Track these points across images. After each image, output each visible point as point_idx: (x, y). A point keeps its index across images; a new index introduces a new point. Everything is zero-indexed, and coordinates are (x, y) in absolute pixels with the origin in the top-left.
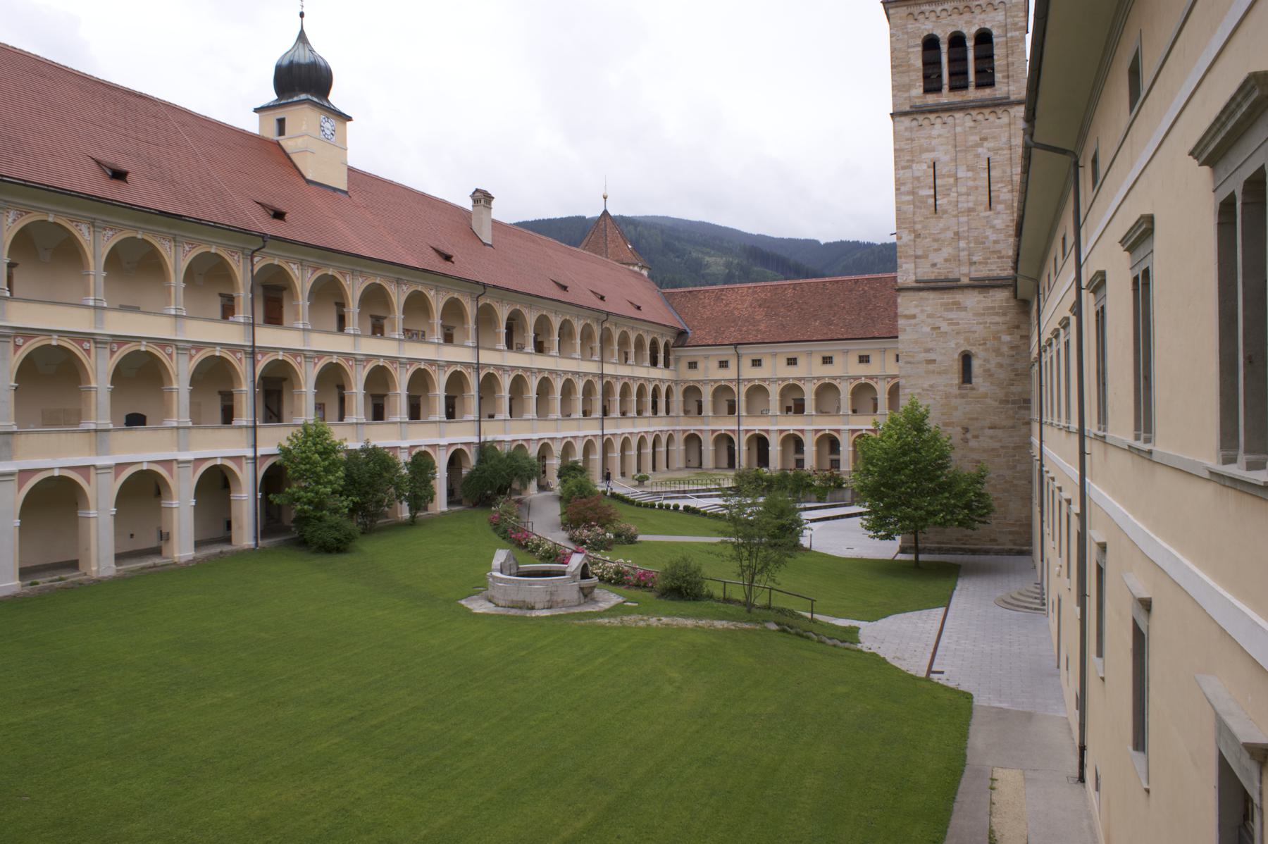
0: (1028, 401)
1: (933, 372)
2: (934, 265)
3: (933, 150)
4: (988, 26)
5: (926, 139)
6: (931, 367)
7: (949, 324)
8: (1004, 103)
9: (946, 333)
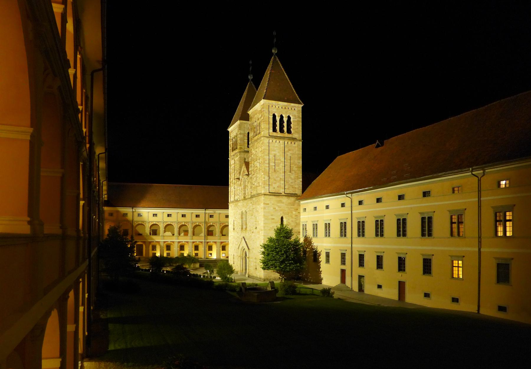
0: (299, 232)
6: (273, 221)
8: (294, 139)
9: (277, 210)
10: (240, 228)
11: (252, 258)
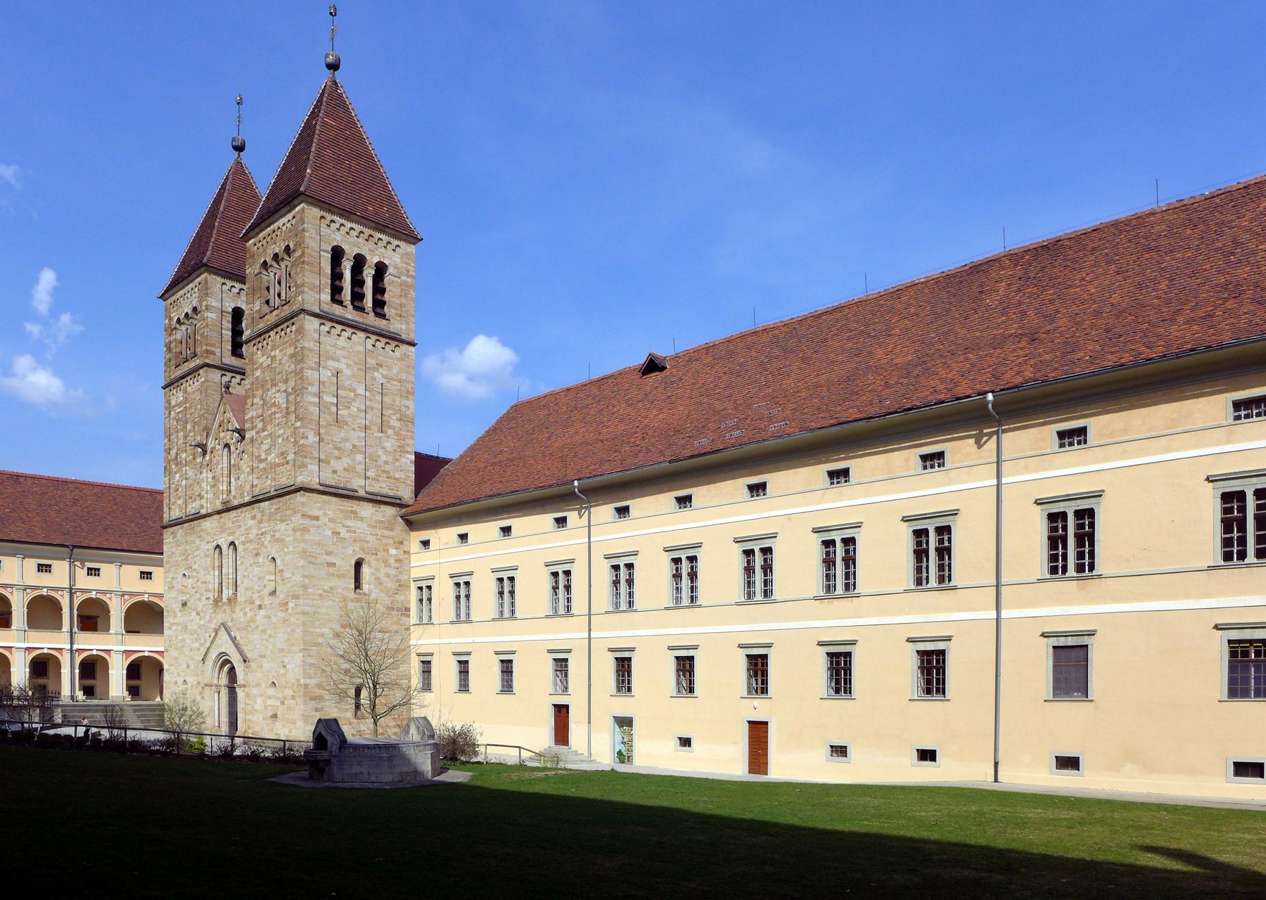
1: (334, 575)
2: (335, 472)
3: (338, 360)
4: (386, 262)
5: (331, 347)
6: (331, 570)
7: (347, 531)
10: (208, 599)
11: (258, 685)
